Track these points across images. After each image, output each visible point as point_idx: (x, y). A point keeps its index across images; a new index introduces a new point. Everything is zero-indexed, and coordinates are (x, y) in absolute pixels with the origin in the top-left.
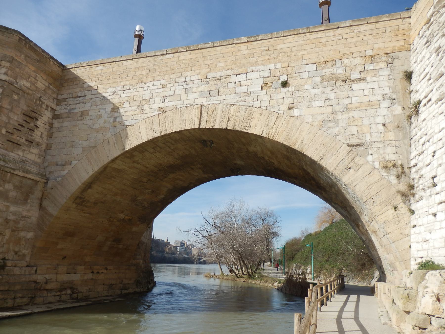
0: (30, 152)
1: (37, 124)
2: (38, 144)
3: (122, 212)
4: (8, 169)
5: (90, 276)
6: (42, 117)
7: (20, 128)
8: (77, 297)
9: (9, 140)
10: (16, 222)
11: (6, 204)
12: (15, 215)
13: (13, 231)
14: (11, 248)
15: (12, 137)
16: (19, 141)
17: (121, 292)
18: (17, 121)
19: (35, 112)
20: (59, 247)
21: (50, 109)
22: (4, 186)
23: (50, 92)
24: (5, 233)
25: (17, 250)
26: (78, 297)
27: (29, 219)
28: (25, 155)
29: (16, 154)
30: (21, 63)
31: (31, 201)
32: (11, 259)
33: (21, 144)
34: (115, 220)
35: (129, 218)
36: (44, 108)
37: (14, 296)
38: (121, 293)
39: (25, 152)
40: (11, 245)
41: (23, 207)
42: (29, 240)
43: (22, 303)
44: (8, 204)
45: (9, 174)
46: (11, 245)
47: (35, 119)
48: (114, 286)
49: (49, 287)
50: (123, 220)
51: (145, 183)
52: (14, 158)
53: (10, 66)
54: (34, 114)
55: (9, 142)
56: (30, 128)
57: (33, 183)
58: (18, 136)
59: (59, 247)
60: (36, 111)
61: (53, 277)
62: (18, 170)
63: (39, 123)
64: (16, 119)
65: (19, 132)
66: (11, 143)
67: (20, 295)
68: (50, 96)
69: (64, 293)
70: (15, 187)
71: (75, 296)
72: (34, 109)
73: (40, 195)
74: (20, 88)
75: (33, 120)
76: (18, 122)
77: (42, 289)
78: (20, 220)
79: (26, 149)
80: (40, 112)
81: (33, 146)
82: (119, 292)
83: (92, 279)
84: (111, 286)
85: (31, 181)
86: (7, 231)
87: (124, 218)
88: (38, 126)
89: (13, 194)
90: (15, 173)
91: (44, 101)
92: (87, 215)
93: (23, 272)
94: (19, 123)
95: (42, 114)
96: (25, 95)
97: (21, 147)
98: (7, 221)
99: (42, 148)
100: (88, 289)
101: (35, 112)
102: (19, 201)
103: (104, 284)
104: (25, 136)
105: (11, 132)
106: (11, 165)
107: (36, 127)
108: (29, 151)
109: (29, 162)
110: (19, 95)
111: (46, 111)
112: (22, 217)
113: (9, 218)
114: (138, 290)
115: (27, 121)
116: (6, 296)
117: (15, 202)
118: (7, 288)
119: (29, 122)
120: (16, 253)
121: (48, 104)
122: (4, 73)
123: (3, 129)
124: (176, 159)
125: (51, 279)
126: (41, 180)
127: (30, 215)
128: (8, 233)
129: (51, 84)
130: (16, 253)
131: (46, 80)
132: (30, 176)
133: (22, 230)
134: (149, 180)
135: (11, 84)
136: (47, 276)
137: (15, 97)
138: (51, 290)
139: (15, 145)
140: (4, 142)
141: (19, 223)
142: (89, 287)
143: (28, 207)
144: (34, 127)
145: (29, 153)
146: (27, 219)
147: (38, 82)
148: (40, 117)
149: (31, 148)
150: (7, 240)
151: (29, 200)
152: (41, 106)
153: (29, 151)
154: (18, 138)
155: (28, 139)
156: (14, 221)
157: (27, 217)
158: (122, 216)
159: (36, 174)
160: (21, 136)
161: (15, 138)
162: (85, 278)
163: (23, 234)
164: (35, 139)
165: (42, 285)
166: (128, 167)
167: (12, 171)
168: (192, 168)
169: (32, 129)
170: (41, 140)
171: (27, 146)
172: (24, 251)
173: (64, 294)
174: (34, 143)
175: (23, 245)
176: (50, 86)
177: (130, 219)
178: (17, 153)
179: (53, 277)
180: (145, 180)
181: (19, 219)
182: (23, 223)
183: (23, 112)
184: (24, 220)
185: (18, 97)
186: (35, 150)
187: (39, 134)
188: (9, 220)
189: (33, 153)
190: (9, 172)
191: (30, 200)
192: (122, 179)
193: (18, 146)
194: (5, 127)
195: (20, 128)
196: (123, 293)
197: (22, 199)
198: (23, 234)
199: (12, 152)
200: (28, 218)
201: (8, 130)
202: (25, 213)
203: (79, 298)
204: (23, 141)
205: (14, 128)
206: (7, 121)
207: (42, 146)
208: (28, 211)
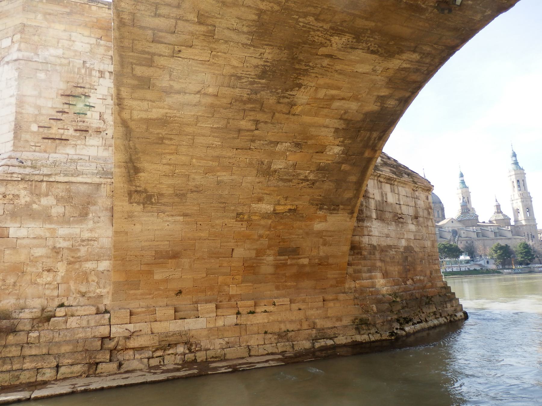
0: (86, 146)
1: (89, 103)
2: (98, 131)
3: (260, 200)
4: (38, 176)
5: (232, 319)
6: (96, 89)
7: (59, 116)
8: (193, 358)
9: (46, 137)
10: (73, 249)
11: (48, 226)
12: (69, 240)
13: (69, 263)
14: (73, 288)
15: (50, 132)
16: (62, 135)
17: (313, 344)
18: (52, 108)
19: (81, 87)
20: (157, 277)
21: (107, 75)
22: (40, 201)
23: (101, 50)
24: (57, 269)
25: (83, 289)
26: (195, 359)
27: (96, 242)
28: (78, 152)
29: (63, 154)
30: (39, 26)
31: (94, 214)
32: (74, 304)
33: (67, 139)
34: (254, 218)
35: (289, 207)
36: (95, 77)
37: (56, 363)
38: (314, 347)
39: (78, 147)
40: (72, 284)
41: (82, 227)
42: (103, 273)
43: (72, 373)
44: (53, 226)
45: (44, 184)
46: (72, 284)
47: (83, 97)
48: (290, 334)
49: (133, 343)
50: (275, 213)
51: (256, 132)
52: (55, 160)
53: (21, 38)
54: (80, 90)
55: (47, 140)
56: (78, 111)
57: (91, 188)
58: (59, 129)
59: (157, 277)
60: (82, 85)
61: (144, 327)
62: (56, 174)
63: (92, 101)
64: (50, 106)
65: (59, 122)
66: (50, 141)
67: (70, 361)
68: (102, 56)
69: (171, 351)
70: (59, 199)
71: (190, 357)
72: (78, 83)
73: (110, 204)
74: (45, 62)
75: (80, 99)
76: (55, 108)
77: (119, 347)
78: (80, 245)
79: (79, 142)
80: (90, 84)
81: (91, 136)
82: (307, 345)
83: (236, 325)
84: (282, 336)
85: (86, 186)
86: (60, 264)
87: (274, 210)
88: (91, 105)
89: (57, 210)
90: (51, 180)
91: (92, 66)
92: (181, 218)
93: (84, 323)
94: (57, 110)
95: (95, 85)
96: (58, 68)
97: (69, 142)
98: (56, 251)
99: (107, 134)
100: (224, 343)
101: (81, 87)
102: (71, 219)
103: (266, 333)
104: (72, 125)
105: (46, 126)
106: (46, 171)
107: (88, 107)
108: (85, 145)
109: (84, 160)
110: (48, 72)
111: (101, 79)
112: (83, 241)
113: (58, 245)
114: (359, 338)
115: (70, 103)
116: (40, 364)
117: (64, 220)
118: (45, 351)
119: (74, 103)
120: (83, 295)
121: (101, 69)
122: (17, 50)
123: (32, 125)
124: (252, 48)
125: (141, 330)
126: (103, 181)
127: (96, 235)
128: (62, 268)
129: (101, 38)
130: (83, 295)
131: (89, 36)
132: (79, 179)
133: (87, 260)
134: (257, 122)
135: (29, 60)
136: (131, 327)
137: (42, 75)
138: (141, 349)
139: (58, 141)
140: (38, 142)
141: (79, 250)
142: (226, 339)
143: (90, 224)
144: (85, 108)
145: (84, 147)
146: (92, 242)
147: (76, 43)
148: (92, 91)
149: (87, 140)
150: (63, 277)
151: (91, 215)
152: (90, 75)
153: (85, 145)
154: (61, 131)
155: (79, 128)
156: (68, 249)
157: (91, 240)
158: (266, 207)
159: (93, 174)
160: (65, 127)
161: (55, 131)
162: (220, 323)
163: (89, 265)
164: (92, 125)
165: (118, 342)
166: (169, 109)
167: (45, 179)
168: (330, 56)
169: (81, 112)
170: (103, 124)
171: (79, 138)
172: (98, 291)
173: (172, 354)
174: (90, 132)
175: (94, 281)
176: (99, 43)
177: (290, 210)
178: (64, 152)
179: (144, 327)
180: (245, 124)
181: (77, 244)
182: (86, 249)
183: (61, 92)
184: (87, 245)
185: (46, 74)
186: (94, 141)
187: (97, 116)
188: (60, 248)
189: (92, 146)
190: (42, 181)
191: (92, 213)
192: (190, 137)
193: (63, 141)
194: (35, 122)
195: (59, 116)
196: (317, 345)
197: (77, 215)
198: (89, 265)
199: (56, 153)
200: (94, 240)
201: (41, 124)
202: (86, 235)
203: (199, 360)
204: (71, 132)
205: (50, 119)
206: (36, 112)
207: (106, 132)
208: (91, 230)
